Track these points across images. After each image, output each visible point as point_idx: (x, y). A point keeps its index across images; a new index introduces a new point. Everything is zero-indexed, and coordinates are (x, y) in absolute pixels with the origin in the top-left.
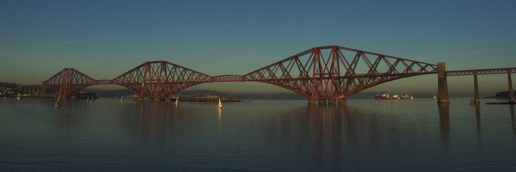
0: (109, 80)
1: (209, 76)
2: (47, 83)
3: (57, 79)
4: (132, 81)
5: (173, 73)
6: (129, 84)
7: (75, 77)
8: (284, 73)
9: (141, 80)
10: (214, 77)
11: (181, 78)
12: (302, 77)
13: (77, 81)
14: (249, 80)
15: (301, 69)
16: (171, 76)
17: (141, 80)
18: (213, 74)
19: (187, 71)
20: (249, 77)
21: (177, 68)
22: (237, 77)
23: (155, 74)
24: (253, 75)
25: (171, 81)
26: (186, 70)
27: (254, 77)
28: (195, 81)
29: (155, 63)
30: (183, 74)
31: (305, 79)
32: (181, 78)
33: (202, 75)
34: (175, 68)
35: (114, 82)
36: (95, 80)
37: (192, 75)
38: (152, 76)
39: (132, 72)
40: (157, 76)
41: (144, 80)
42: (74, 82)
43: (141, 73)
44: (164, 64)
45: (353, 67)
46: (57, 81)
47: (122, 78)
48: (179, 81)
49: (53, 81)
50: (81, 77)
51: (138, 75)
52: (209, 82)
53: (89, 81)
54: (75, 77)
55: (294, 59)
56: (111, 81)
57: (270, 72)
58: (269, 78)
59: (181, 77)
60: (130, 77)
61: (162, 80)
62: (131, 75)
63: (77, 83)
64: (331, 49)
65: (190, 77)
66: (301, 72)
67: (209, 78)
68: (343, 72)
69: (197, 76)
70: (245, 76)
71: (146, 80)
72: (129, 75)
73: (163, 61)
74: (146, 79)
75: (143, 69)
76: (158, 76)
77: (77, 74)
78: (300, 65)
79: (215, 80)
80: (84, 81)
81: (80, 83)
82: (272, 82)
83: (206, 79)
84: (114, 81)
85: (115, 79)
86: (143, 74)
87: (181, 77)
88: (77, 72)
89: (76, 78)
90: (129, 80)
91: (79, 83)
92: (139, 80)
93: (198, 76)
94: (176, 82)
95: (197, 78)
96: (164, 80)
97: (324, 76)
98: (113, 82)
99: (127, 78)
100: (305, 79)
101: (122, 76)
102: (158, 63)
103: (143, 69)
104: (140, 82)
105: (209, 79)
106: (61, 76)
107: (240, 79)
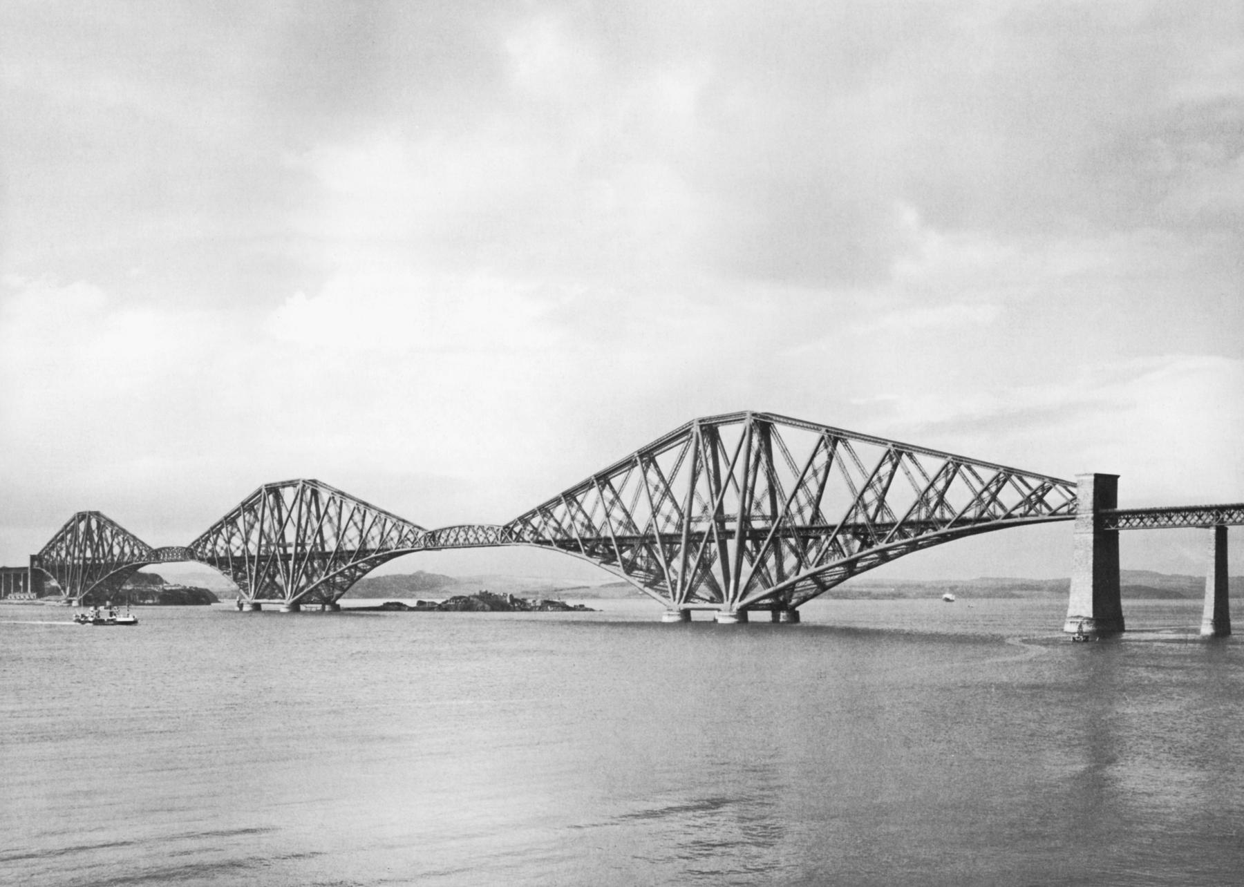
0: (491, 528)
3: (239, 530)
5: (815, 473)
9: (668, 519)
16: (808, 491)
17: (668, 519)
21: (839, 444)
28: (970, 514)
30: (880, 480)
33: (1014, 478)
35: (518, 535)
37: (940, 485)
39: (616, 481)
48: (861, 519)
50: (357, 517)
51: (652, 490)
53: (395, 534)
54: (330, 520)
59: (870, 496)
63: (339, 547)
65: (932, 493)
67: (1070, 497)
69: (979, 488)
75: (682, 458)
80: (369, 537)
81: (352, 544)
85: (524, 520)
86: (680, 488)
87: (870, 496)
89: (335, 520)
91: (349, 547)
92: (661, 520)
95: (979, 497)
98: (514, 536)
99: (583, 512)
103: (682, 458)
104: (664, 527)
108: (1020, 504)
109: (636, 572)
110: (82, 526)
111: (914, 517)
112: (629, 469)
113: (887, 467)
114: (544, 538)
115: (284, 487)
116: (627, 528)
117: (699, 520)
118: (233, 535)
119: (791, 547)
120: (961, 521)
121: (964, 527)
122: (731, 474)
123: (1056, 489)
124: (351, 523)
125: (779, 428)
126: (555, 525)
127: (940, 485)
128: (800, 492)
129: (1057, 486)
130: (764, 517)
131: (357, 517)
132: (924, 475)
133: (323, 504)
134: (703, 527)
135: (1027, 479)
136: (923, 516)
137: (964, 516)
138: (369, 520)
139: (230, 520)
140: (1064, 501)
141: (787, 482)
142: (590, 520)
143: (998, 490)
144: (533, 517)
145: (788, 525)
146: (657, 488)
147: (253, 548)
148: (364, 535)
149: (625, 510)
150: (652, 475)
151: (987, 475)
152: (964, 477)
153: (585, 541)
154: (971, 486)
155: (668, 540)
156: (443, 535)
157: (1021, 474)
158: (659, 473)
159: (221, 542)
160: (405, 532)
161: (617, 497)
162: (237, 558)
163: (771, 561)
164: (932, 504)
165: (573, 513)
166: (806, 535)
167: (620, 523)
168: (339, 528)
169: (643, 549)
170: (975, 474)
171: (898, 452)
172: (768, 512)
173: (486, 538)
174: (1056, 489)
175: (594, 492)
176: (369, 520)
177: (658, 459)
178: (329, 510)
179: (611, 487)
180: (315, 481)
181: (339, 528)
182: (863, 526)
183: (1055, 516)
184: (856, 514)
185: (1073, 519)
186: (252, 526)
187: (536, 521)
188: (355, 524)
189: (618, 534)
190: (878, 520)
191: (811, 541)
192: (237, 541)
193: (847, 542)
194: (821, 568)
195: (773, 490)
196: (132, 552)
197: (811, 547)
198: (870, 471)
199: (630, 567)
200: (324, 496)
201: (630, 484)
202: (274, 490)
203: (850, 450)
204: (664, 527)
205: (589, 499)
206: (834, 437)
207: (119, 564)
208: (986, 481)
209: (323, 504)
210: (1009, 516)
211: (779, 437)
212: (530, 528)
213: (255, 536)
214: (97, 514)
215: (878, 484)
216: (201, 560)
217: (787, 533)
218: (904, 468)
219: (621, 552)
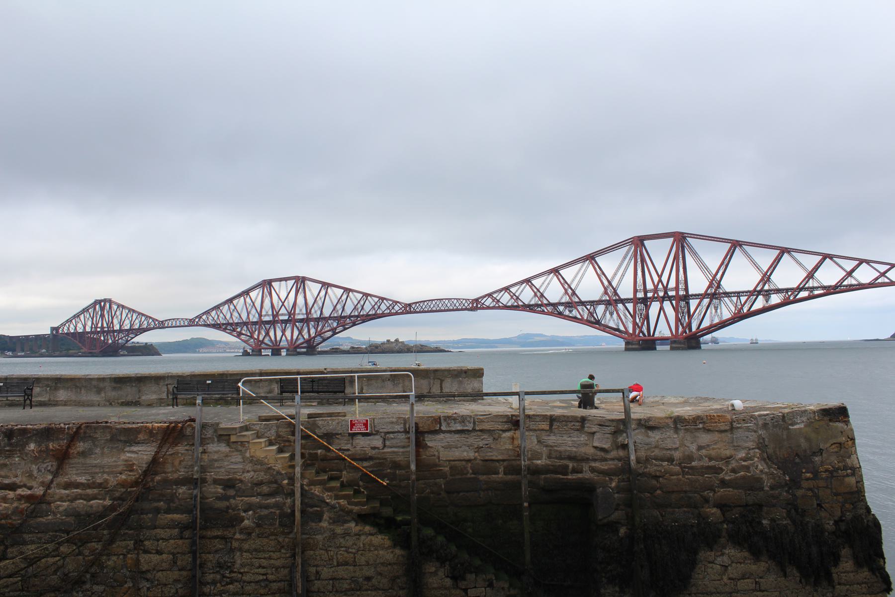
0: (187, 319)
1: (398, 302)
2: (61, 329)
4: (234, 318)
5: (321, 299)
8: (566, 290)
9: (254, 316)
10: (410, 305)
11: (340, 309)
12: (608, 298)
14: (488, 308)
15: (606, 283)
16: (318, 305)
17: (254, 316)
18: (406, 296)
20: (489, 302)
22: (462, 302)
23: (283, 305)
24: (497, 296)
26: (349, 293)
27: (498, 301)
28: (370, 313)
29: (282, 282)
30: (342, 301)
31: (612, 301)
32: (340, 309)
33: (385, 301)
34: (324, 289)
35: (197, 322)
36: (157, 320)
37: (362, 303)
38: (278, 306)
39: (235, 302)
40: (287, 308)
41: (260, 315)
44: (300, 282)
45: (718, 277)
47: (213, 313)
48: (336, 315)
49: (72, 326)
50: (129, 316)
51: (248, 305)
52: (402, 313)
55: (588, 261)
56: (191, 320)
57: (535, 290)
58: (533, 302)
59: (339, 307)
61: (299, 314)
62: (232, 307)
64: (672, 239)
65: (359, 305)
66: (606, 289)
67: (401, 307)
68: (698, 283)
69: (373, 304)
70: (477, 300)
71: (265, 316)
72: (229, 306)
74: (264, 313)
75: (258, 294)
76: (289, 307)
77: (120, 309)
78: (601, 274)
79: (412, 309)
81: (127, 326)
82: (539, 309)
83: (393, 308)
84: (197, 320)
85: (199, 317)
86: (258, 304)
87: (339, 307)
88: (119, 306)
89: (120, 317)
91: (126, 328)
93: (376, 303)
94: (330, 318)
95: (373, 307)
96: (303, 314)
97: (658, 294)
98: (196, 323)
100: (612, 301)
102: (288, 282)
103: (258, 294)
104: (253, 319)
105: (401, 309)
106: (88, 316)
107: (468, 305)
111: (353, 314)
113: (344, 297)
116: (239, 320)
119: (312, 325)
120: (367, 315)
121: (368, 318)
124: (127, 318)
125: (308, 283)
127: (362, 303)
128: (315, 305)
131: (129, 316)
132: (357, 299)
133: (114, 310)
136: (356, 314)
141: (310, 301)
143: (380, 305)
146: (250, 305)
147: (88, 329)
148: (132, 323)
149: (238, 313)
150: (248, 300)
153: (223, 324)
154: (371, 304)
157: (387, 300)
158: (251, 300)
160: (150, 322)
163: (306, 331)
164: (359, 311)
165: (218, 314)
166: (317, 320)
167: (237, 318)
169: (245, 326)
170: (373, 299)
173: (184, 323)
175: (226, 306)
177: (250, 294)
178: (117, 313)
179: (233, 304)
182: (336, 317)
184: (334, 313)
187: (204, 317)
188: (129, 318)
189: (236, 322)
190: (342, 315)
199: (239, 335)
200: (115, 307)
204: (253, 319)
206: (326, 285)
208: (376, 301)
209: (114, 310)
210: (383, 313)
211: (308, 287)
212: (202, 320)
213: (89, 323)
219: (237, 329)
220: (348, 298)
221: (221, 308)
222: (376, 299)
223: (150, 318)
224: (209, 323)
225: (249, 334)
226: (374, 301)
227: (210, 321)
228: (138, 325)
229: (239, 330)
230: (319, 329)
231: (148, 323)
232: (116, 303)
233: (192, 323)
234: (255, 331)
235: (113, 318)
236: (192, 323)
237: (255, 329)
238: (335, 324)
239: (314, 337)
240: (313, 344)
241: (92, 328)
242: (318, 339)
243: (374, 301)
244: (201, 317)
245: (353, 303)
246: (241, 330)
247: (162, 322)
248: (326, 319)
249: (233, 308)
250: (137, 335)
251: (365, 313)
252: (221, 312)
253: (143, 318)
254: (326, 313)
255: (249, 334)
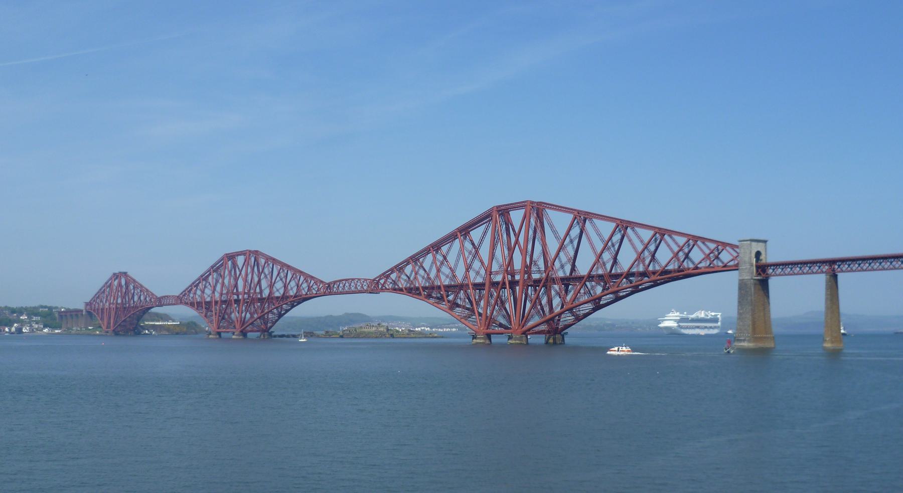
0: (366, 280)
4: (443, 277)
5: (571, 241)
6: (432, 288)
7: (266, 276)
9: (478, 273)
13: (271, 286)
16: (566, 254)
17: (478, 273)
19: (629, 230)
25: (564, 272)
28: (670, 267)
30: (613, 245)
33: (699, 243)
35: (383, 285)
36: (321, 282)
37: (652, 248)
39: (444, 249)
42: (261, 292)
43: (477, 249)
46: (199, 292)
47: (408, 269)
48: (600, 272)
50: (282, 275)
51: (467, 254)
53: (305, 285)
59: (607, 256)
60: (438, 264)
65: (646, 253)
67: (735, 254)
69: (676, 249)
72: (435, 258)
73: (532, 203)
75: (485, 233)
84: (382, 281)
85: (386, 275)
88: (268, 259)
89: (269, 277)
90: (432, 275)
91: (277, 294)
92: (472, 274)
93: (681, 249)
94: (590, 277)
95: (676, 255)
98: (380, 286)
101: (408, 264)
103: (485, 233)
104: (475, 278)
108: (703, 260)
109: (458, 309)
110: (116, 283)
111: (634, 270)
112: (452, 241)
113: (617, 237)
114: (398, 286)
115: (238, 255)
116: (451, 280)
117: (497, 273)
118: (205, 287)
119: (556, 291)
120: (664, 272)
121: (666, 276)
122: (517, 242)
123: (727, 250)
124: (278, 278)
125: (550, 213)
126: (405, 278)
127: (652, 248)
128: (562, 254)
129: (728, 248)
130: (539, 271)
132: (642, 241)
134: (499, 278)
135: (708, 244)
136: (641, 268)
137: (666, 268)
138: (289, 276)
139: (204, 278)
140: (731, 258)
141: (553, 246)
142: (428, 275)
143: (690, 251)
144: (392, 273)
145: (554, 276)
146: (470, 253)
147: (217, 295)
150: (468, 245)
151: (682, 240)
152: (666, 243)
153: (424, 288)
154: (671, 249)
155: (479, 287)
156: (335, 286)
157: (704, 240)
158: (473, 244)
159: (199, 292)
161: (445, 258)
162: (208, 302)
164: (647, 262)
166: (566, 282)
168: (271, 282)
170: (674, 240)
171: (623, 226)
172: (542, 268)
173: (362, 287)
174: (727, 250)
175: (430, 257)
176: (289, 276)
180: (257, 251)
181: (271, 282)
183: (726, 268)
184: (597, 268)
185: (737, 270)
186: (217, 281)
187: (393, 276)
188: (281, 279)
190: (613, 271)
191: (570, 286)
192: (208, 291)
193: (592, 287)
194: (243, 327)
195: (545, 253)
196: (145, 299)
197: (570, 292)
198: (606, 238)
201: (453, 250)
202: (232, 257)
203: (594, 226)
205: (428, 261)
207: (136, 307)
208: (681, 244)
210: (696, 268)
214: (125, 274)
215: (612, 247)
216: (186, 304)
217: (554, 281)
218: (628, 237)
219: (448, 296)
220: (625, 238)
221: (421, 260)
222: (682, 240)
223: (312, 278)
224: (401, 286)
225: (468, 306)
226: (676, 243)
227: (402, 284)
228: (295, 290)
229: (451, 298)
230: (569, 298)
231: (309, 286)
232: (263, 255)
233: (375, 287)
234: (480, 300)
235: (236, 279)
236: (375, 287)
237: (480, 296)
238: (599, 290)
239: (560, 315)
240: (558, 324)
241: (221, 294)
242: (568, 318)
243: (676, 243)
244: (388, 277)
245: (593, 248)
246: (456, 296)
247: (329, 284)
248: (580, 278)
249: (441, 258)
250: (293, 306)
251: (657, 268)
252: (422, 267)
253: (302, 279)
254: (583, 269)
255: (468, 306)
